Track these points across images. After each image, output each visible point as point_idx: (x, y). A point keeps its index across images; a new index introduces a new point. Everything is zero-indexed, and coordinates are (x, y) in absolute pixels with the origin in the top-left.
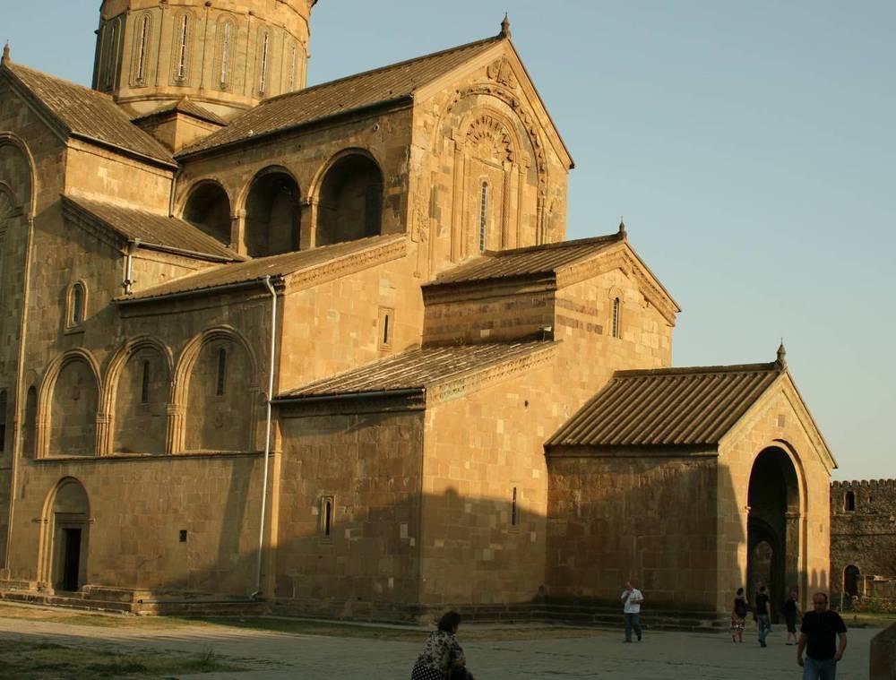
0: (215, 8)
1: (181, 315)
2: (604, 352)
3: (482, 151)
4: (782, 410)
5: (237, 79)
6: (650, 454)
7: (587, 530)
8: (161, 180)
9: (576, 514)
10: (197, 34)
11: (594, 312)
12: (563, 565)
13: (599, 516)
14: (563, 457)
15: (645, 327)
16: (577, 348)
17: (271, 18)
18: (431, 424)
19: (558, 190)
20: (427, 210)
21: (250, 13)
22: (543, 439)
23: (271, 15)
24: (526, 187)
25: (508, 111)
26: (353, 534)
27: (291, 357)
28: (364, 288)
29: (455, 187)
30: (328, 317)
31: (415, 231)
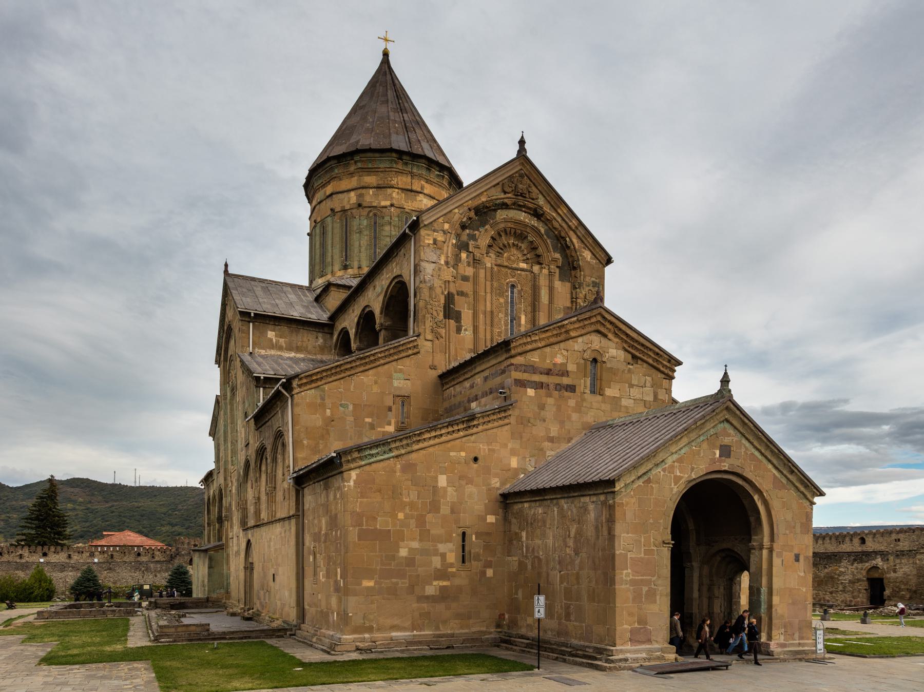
0: (365, 207)
2: (578, 409)
3: (509, 259)
11: (565, 373)
15: (634, 382)
16: (542, 407)
18: (352, 483)
19: (593, 282)
20: (442, 314)
21: (392, 205)
22: (498, 489)
23: (410, 204)
24: (557, 284)
28: (376, 383)
29: (475, 292)
31: (428, 331)
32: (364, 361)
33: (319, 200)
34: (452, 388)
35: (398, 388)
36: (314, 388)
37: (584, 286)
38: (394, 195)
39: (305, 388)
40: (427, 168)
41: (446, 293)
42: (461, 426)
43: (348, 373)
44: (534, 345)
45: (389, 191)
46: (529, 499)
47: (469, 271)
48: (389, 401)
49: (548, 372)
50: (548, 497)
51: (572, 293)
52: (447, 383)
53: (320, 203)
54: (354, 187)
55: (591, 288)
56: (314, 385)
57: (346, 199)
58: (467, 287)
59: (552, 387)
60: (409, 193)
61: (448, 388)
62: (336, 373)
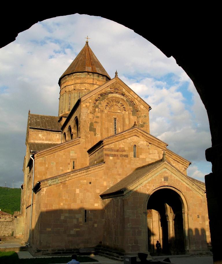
2: (129, 163)
3: (114, 110)
4: (166, 175)
8: (58, 135)
11: (124, 151)
15: (151, 152)
16: (115, 163)
18: (44, 192)
19: (145, 116)
22: (99, 193)
24: (132, 117)
25: (122, 97)
27: (38, 176)
28: (64, 154)
29: (101, 122)
30: (51, 164)
35: (72, 156)
37: (141, 117)
38: (86, 86)
41: (90, 122)
42: (84, 171)
43: (54, 152)
44: (112, 142)
45: (84, 84)
47: (99, 115)
48: (69, 161)
49: (118, 151)
54: (73, 84)
55: (144, 118)
57: (70, 88)
58: (98, 120)
59: (119, 156)
62: (50, 152)
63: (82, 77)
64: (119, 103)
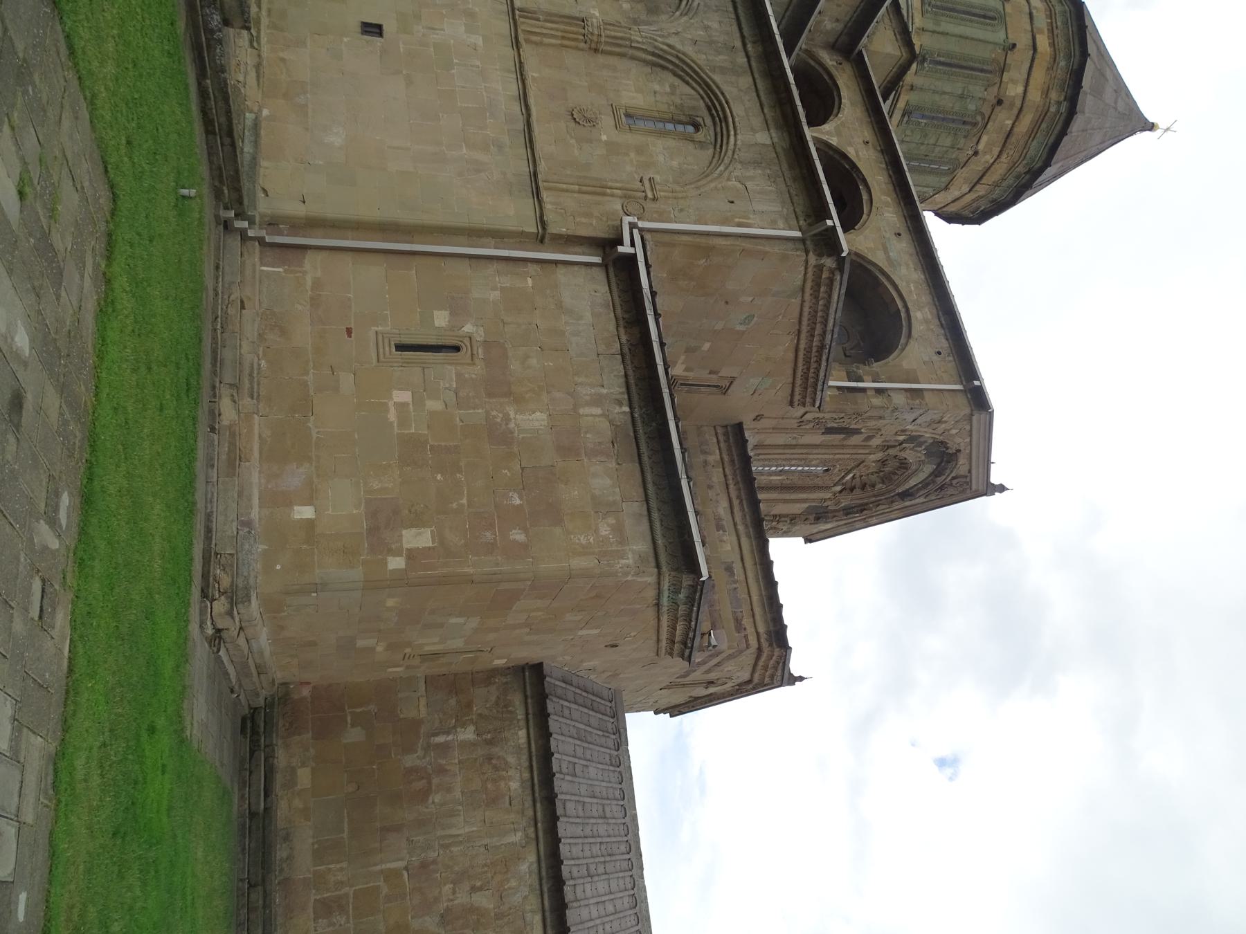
0: (993, 109)
1: (743, 54)
5: (912, 131)
6: (544, 873)
7: (410, 761)
8: (840, 26)
9: (436, 735)
10: (971, 88)
12: (349, 719)
13: (435, 781)
14: (526, 697)
17: (962, 174)
24: (806, 505)
26: (401, 406)
32: (814, 353)
33: (1034, 12)
34: (719, 457)
36: (804, 285)
39: (810, 275)
40: (996, 200)
41: (862, 430)
45: (996, 151)
46: (533, 749)
50: (539, 814)
51: (786, 516)
52: (726, 434)
53: (1031, 14)
54: (1028, 94)
56: (809, 284)
60: (980, 174)
61: (718, 442)
63: (1035, 141)
64: (878, 480)
